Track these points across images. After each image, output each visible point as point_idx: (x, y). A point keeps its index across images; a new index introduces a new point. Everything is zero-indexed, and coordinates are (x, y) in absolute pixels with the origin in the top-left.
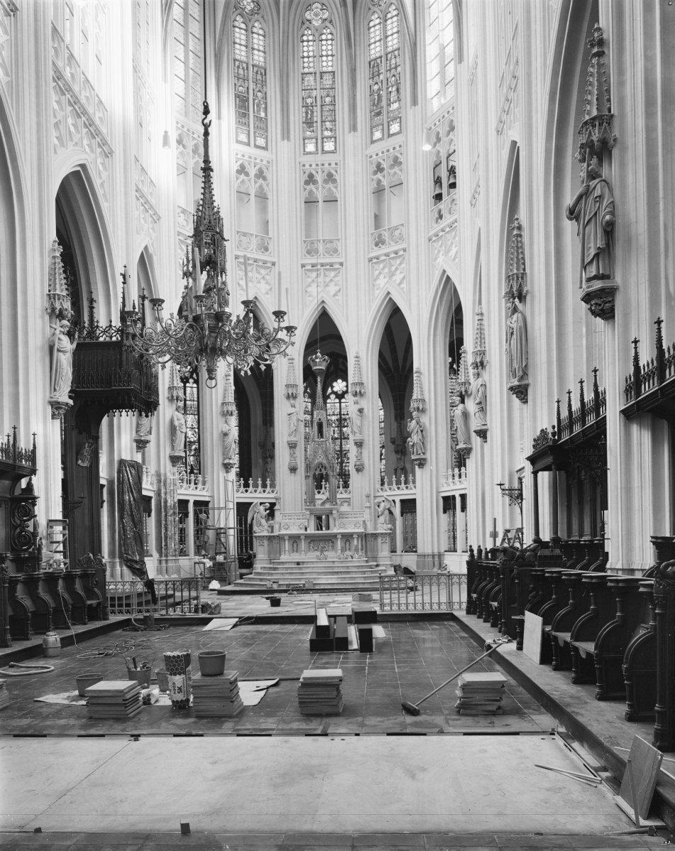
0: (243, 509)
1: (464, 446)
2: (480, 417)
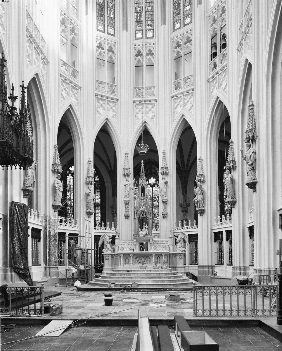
0: (97, 238)
1: (232, 200)
2: (251, 174)
